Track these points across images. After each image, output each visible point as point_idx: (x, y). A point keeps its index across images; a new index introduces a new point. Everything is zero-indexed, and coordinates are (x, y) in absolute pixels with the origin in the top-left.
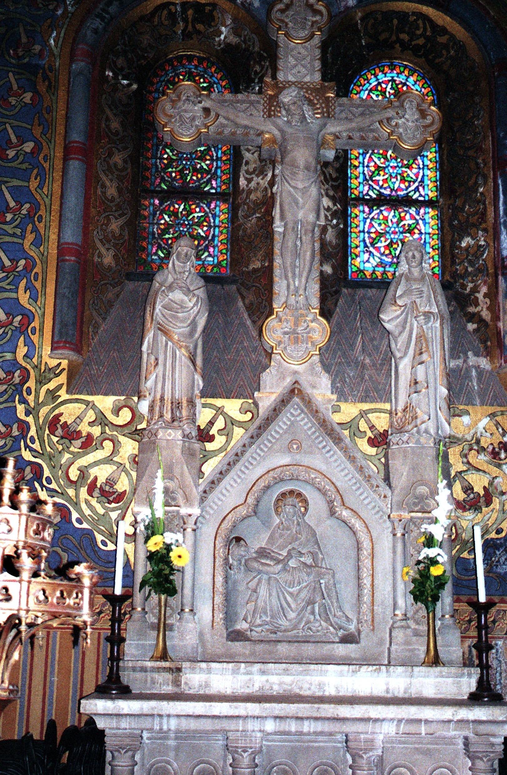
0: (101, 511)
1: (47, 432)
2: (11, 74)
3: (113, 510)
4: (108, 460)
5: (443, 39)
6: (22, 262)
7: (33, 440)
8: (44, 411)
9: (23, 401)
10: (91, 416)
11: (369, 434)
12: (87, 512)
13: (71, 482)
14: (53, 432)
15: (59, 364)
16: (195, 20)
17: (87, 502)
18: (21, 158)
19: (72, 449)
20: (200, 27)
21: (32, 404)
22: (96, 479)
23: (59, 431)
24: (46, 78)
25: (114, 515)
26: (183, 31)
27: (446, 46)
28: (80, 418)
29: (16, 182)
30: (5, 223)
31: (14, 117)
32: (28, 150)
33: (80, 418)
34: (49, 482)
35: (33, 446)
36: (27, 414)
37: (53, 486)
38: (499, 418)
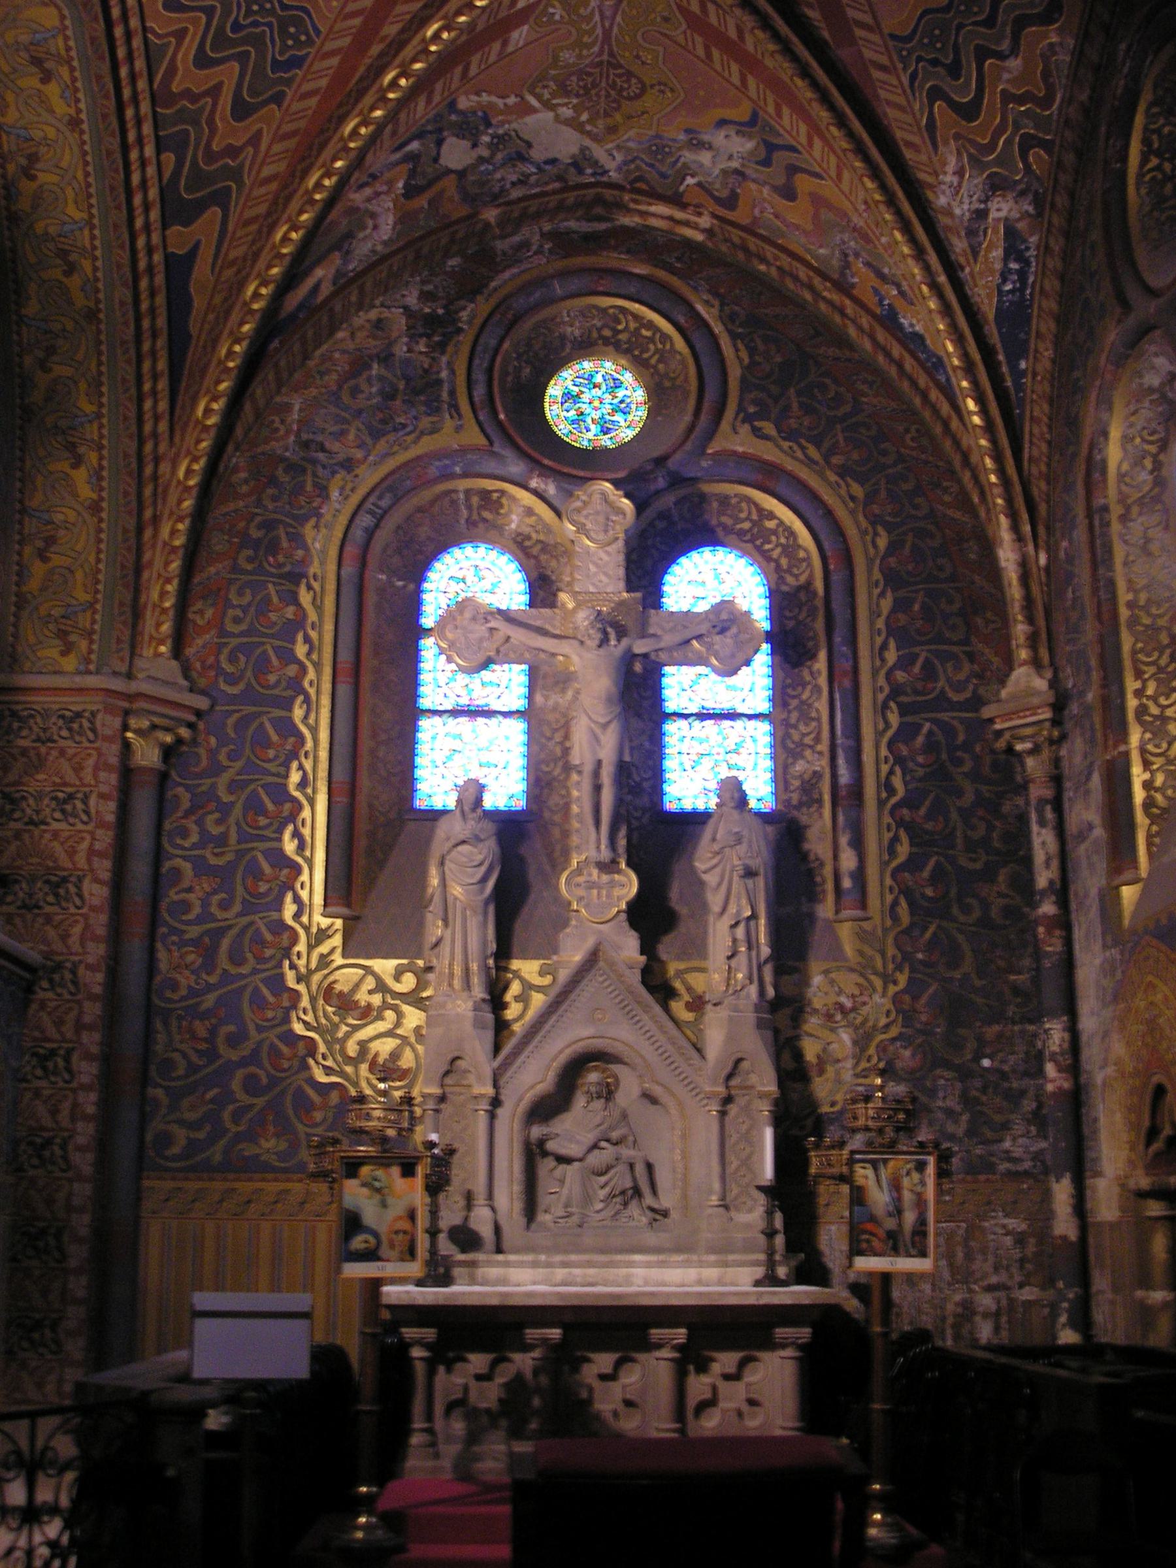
1: (321, 1002)
2: (270, 586)
4: (390, 1034)
5: (771, 524)
7: (305, 1011)
8: (316, 978)
9: (293, 967)
10: (370, 983)
11: (687, 997)
14: (327, 1001)
16: (480, 507)
18: (284, 684)
20: (486, 514)
21: (303, 970)
22: (376, 1055)
23: (335, 1001)
26: (467, 520)
27: (774, 532)
28: (357, 986)
29: (278, 713)
30: (269, 761)
31: (273, 636)
33: (357, 986)
34: (324, 1057)
37: (329, 1063)
38: (833, 975)
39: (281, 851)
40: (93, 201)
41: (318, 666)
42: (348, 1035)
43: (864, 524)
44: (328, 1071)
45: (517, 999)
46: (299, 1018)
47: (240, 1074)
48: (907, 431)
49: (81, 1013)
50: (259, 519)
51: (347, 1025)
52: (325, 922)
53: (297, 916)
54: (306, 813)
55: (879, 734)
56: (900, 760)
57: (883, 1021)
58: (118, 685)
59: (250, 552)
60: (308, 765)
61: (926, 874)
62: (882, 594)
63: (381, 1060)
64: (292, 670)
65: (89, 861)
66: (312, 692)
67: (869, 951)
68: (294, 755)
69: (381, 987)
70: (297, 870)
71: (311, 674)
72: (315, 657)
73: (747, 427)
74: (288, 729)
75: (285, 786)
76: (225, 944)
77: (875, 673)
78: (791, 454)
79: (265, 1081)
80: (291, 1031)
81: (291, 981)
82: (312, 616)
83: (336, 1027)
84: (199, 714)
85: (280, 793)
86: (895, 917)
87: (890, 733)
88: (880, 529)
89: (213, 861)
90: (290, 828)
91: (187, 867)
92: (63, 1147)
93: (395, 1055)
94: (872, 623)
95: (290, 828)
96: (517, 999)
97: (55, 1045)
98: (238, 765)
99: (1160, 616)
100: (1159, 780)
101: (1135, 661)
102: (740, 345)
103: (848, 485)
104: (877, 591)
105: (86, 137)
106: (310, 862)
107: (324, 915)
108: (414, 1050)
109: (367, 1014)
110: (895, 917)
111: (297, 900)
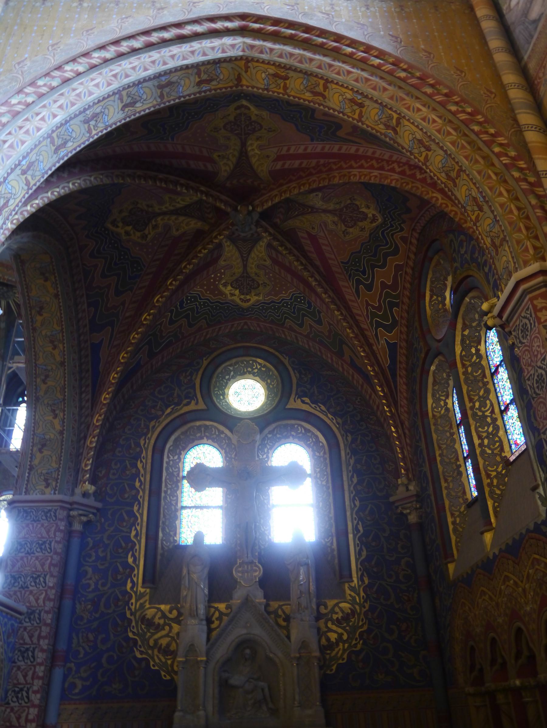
0: (163, 660)
1: (140, 623)
2: (127, 461)
3: (169, 659)
4: (167, 635)
6: (130, 544)
8: (138, 614)
9: (130, 609)
10: (159, 614)
12: (157, 661)
13: (150, 646)
14: (142, 623)
15: (146, 591)
17: (158, 656)
19: (151, 631)
22: (161, 645)
24: (141, 462)
25: (169, 662)
28: (154, 616)
29: (128, 508)
32: (134, 494)
34: (140, 647)
35: (134, 630)
36: (131, 615)
37: (142, 649)
39: (127, 562)
40: (63, 323)
41: (144, 491)
42: (150, 637)
43: (343, 432)
44: (142, 653)
45: (217, 619)
46: (130, 630)
47: (105, 656)
48: (357, 399)
49: (41, 631)
50: (123, 437)
51: (150, 632)
52: (142, 590)
53: (132, 588)
54: (137, 547)
55: (352, 509)
56: (360, 519)
57: (361, 623)
58: (67, 498)
59: (120, 449)
60: (138, 528)
61: (373, 563)
62: (351, 458)
63: (163, 647)
64: (134, 492)
65: (49, 568)
66: (141, 500)
67: (353, 594)
68: (134, 524)
69: (164, 616)
70: (133, 569)
71: (141, 493)
72: (143, 487)
73: (299, 400)
74: (131, 514)
75: (130, 537)
76: (103, 600)
77: (349, 486)
78: (315, 409)
79: (116, 658)
80: (128, 636)
81: (128, 615)
82: (142, 471)
83: (145, 634)
84: (98, 509)
85: (127, 539)
86: (362, 581)
87: (356, 509)
88: (349, 434)
89: (101, 567)
90: (131, 553)
91: (90, 570)
92: (27, 693)
93: (168, 645)
94: (347, 469)
95: (131, 553)
96: (217, 619)
97: (28, 646)
98: (112, 529)
99: (452, 458)
100: (458, 520)
101: (444, 476)
102: (296, 372)
103: (336, 419)
104: (348, 457)
105: (61, 300)
106: (138, 566)
107: (142, 587)
108: (176, 642)
109: (159, 628)
110: (362, 581)
111: (132, 581)
